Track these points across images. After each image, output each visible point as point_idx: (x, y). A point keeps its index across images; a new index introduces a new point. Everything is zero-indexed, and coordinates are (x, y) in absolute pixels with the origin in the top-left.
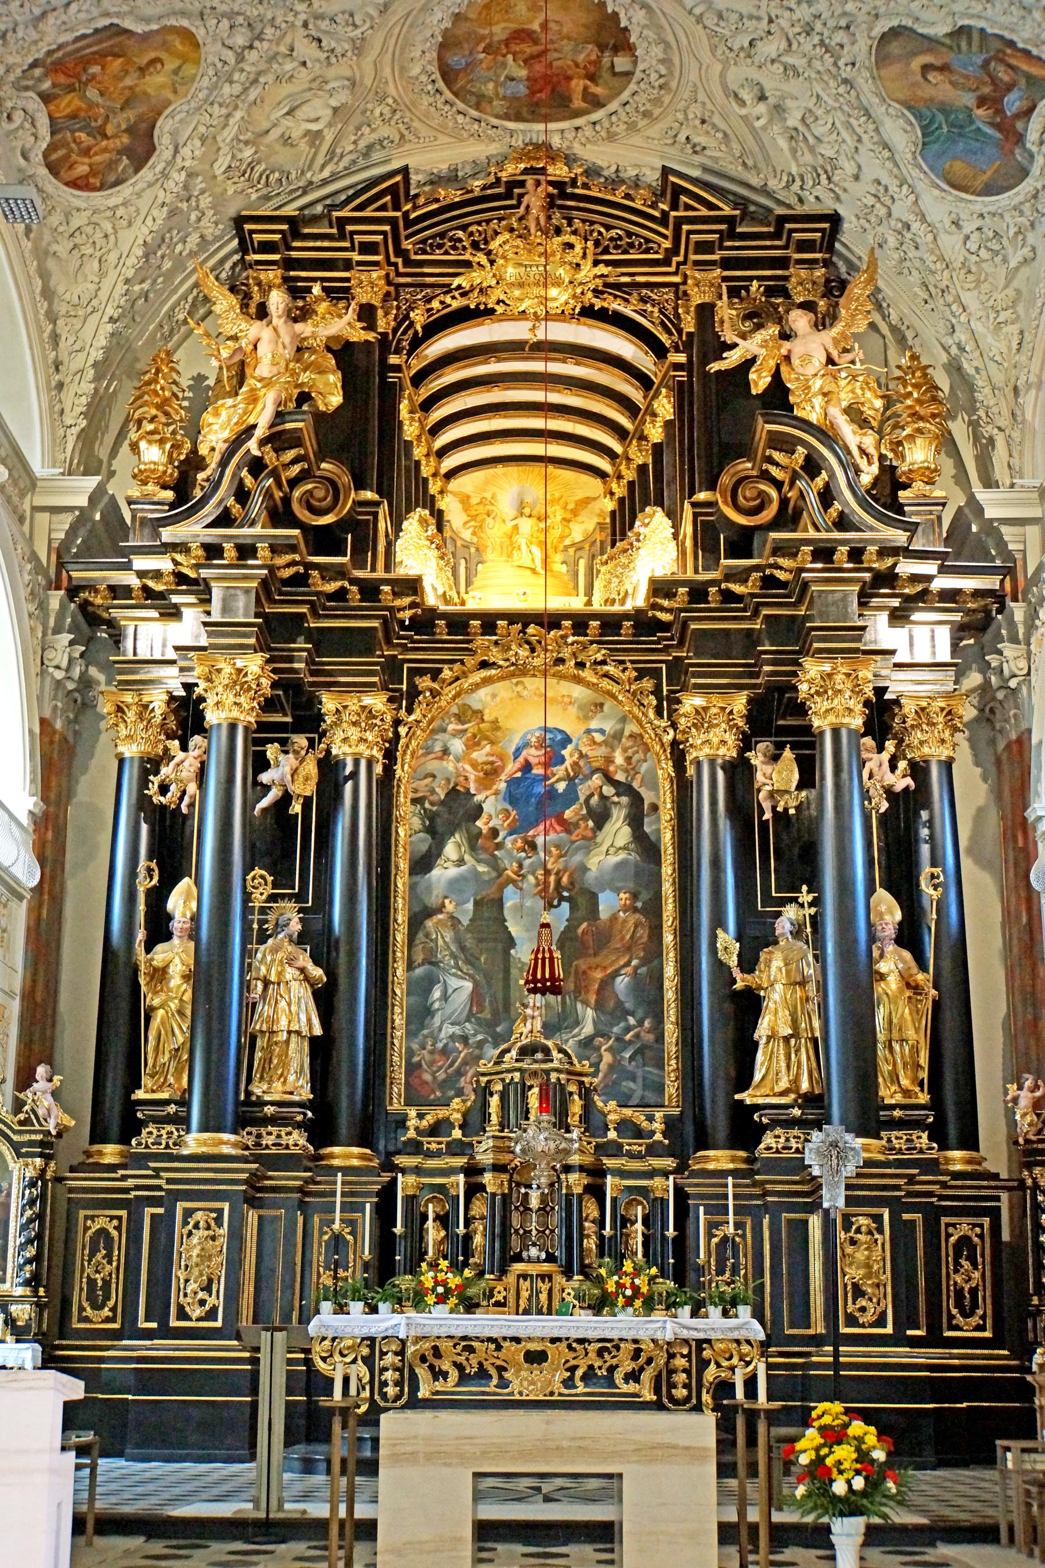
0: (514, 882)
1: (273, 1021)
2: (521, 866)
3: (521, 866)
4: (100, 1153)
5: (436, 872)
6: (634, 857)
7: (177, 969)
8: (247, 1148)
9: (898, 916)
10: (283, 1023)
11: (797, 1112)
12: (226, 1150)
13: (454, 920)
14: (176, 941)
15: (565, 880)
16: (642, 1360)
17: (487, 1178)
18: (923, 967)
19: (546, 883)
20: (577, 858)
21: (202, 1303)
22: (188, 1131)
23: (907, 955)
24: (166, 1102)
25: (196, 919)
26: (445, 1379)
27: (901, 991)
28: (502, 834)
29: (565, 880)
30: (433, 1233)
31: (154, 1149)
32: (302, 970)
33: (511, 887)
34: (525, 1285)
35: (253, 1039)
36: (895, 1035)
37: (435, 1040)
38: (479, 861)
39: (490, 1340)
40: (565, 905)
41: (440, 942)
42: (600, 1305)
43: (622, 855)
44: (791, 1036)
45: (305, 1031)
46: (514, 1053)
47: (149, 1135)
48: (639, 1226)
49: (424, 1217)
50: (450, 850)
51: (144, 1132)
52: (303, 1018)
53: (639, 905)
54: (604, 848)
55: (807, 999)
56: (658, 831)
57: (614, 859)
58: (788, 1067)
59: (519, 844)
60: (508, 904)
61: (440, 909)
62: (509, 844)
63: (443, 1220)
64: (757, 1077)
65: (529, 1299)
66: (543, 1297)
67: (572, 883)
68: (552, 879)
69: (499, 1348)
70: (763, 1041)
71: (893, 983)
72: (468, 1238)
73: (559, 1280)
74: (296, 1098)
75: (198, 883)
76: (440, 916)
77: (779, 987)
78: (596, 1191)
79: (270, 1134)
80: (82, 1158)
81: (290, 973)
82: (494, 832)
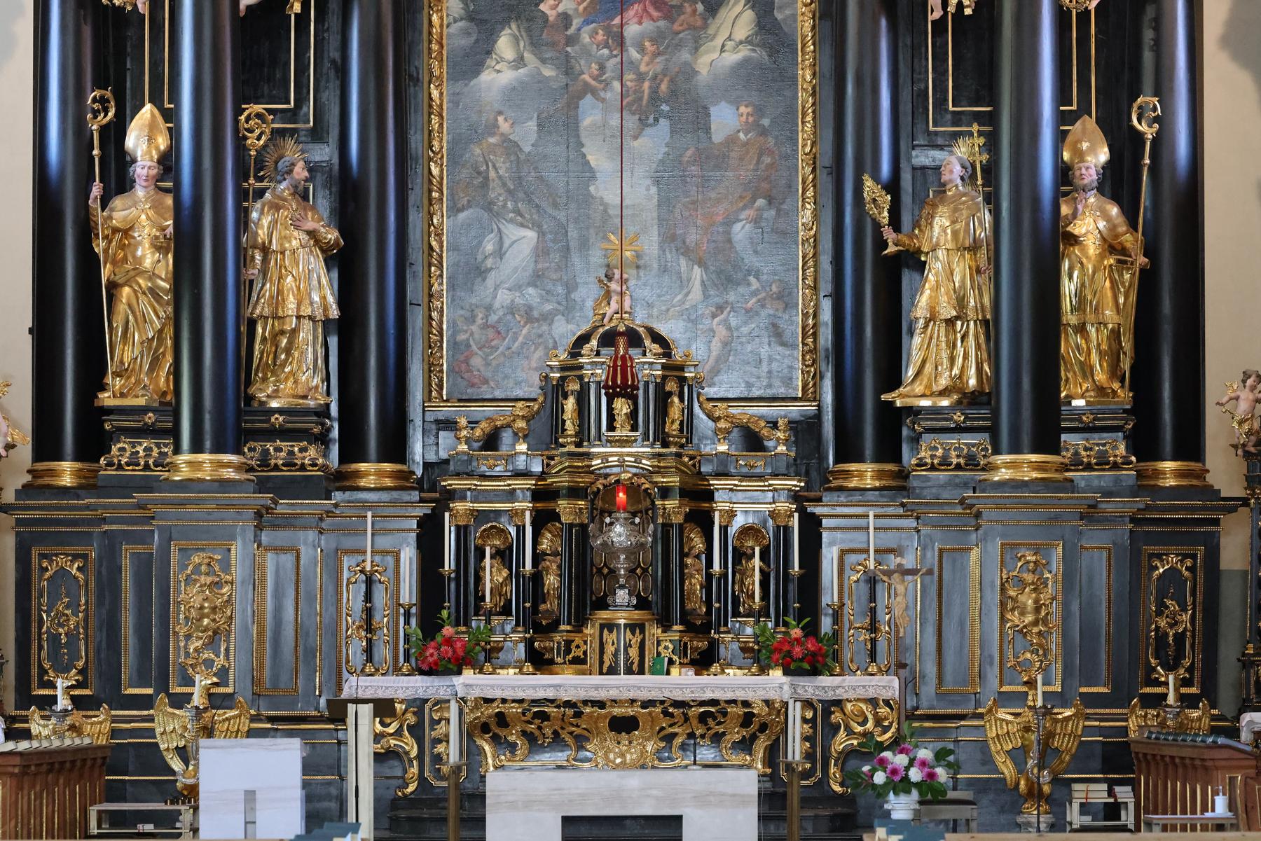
0: (594, 92)
1: (278, 300)
2: (602, 68)
3: (602, 68)
4: (53, 473)
5: (486, 77)
6: (761, 55)
7: (145, 233)
8: (250, 469)
9: (1103, 155)
10: (291, 305)
11: (959, 417)
12: (229, 474)
13: (510, 147)
14: (140, 192)
15: (664, 87)
16: (754, 727)
17: (563, 505)
18: (1133, 225)
19: (638, 91)
20: (685, 56)
21: (209, 663)
22: (177, 451)
23: (1114, 210)
24: (143, 410)
25: (168, 163)
26: (513, 752)
27: (1101, 257)
28: (576, 22)
29: (664, 87)
30: (492, 575)
31: (128, 473)
32: (312, 234)
33: (589, 96)
34: (609, 638)
35: (252, 324)
36: (1091, 317)
37: (489, 308)
38: (543, 61)
39: (568, 704)
40: (663, 122)
41: (492, 174)
42: (704, 661)
43: (744, 52)
44: (957, 318)
45: (319, 315)
46: (594, 342)
47: (121, 450)
48: (757, 562)
49: (481, 554)
50: (505, 45)
51: (114, 449)
52: (316, 298)
53: (766, 122)
54: (719, 41)
55: (978, 271)
56: (794, 16)
57: (732, 58)
58: (952, 360)
59: (601, 36)
60: (586, 122)
61: (493, 128)
62: (585, 38)
63: (503, 555)
64: (911, 372)
65: (616, 655)
66: (634, 653)
67: (673, 93)
68: (646, 85)
69: (578, 715)
70: (921, 323)
71: (1092, 246)
72: (537, 578)
73: (655, 631)
74: (312, 403)
75: (170, 116)
76: (492, 140)
77: (941, 254)
78: (702, 520)
79: (278, 450)
80: (28, 478)
81: (297, 239)
82: (566, 19)
